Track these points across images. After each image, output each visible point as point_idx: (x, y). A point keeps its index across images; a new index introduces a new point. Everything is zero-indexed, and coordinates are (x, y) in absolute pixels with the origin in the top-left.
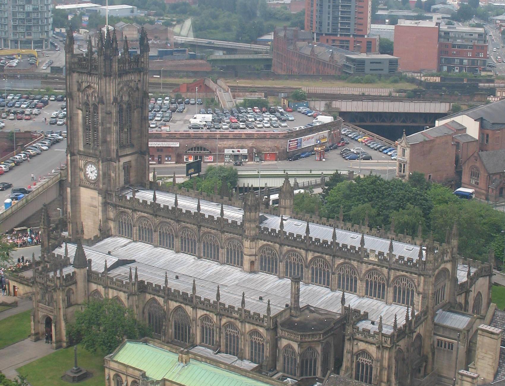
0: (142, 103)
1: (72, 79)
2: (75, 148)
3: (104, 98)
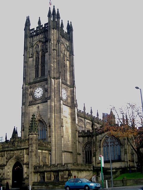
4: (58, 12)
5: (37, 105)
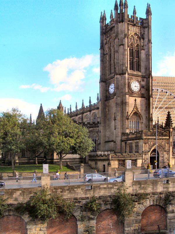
5: (134, 98)
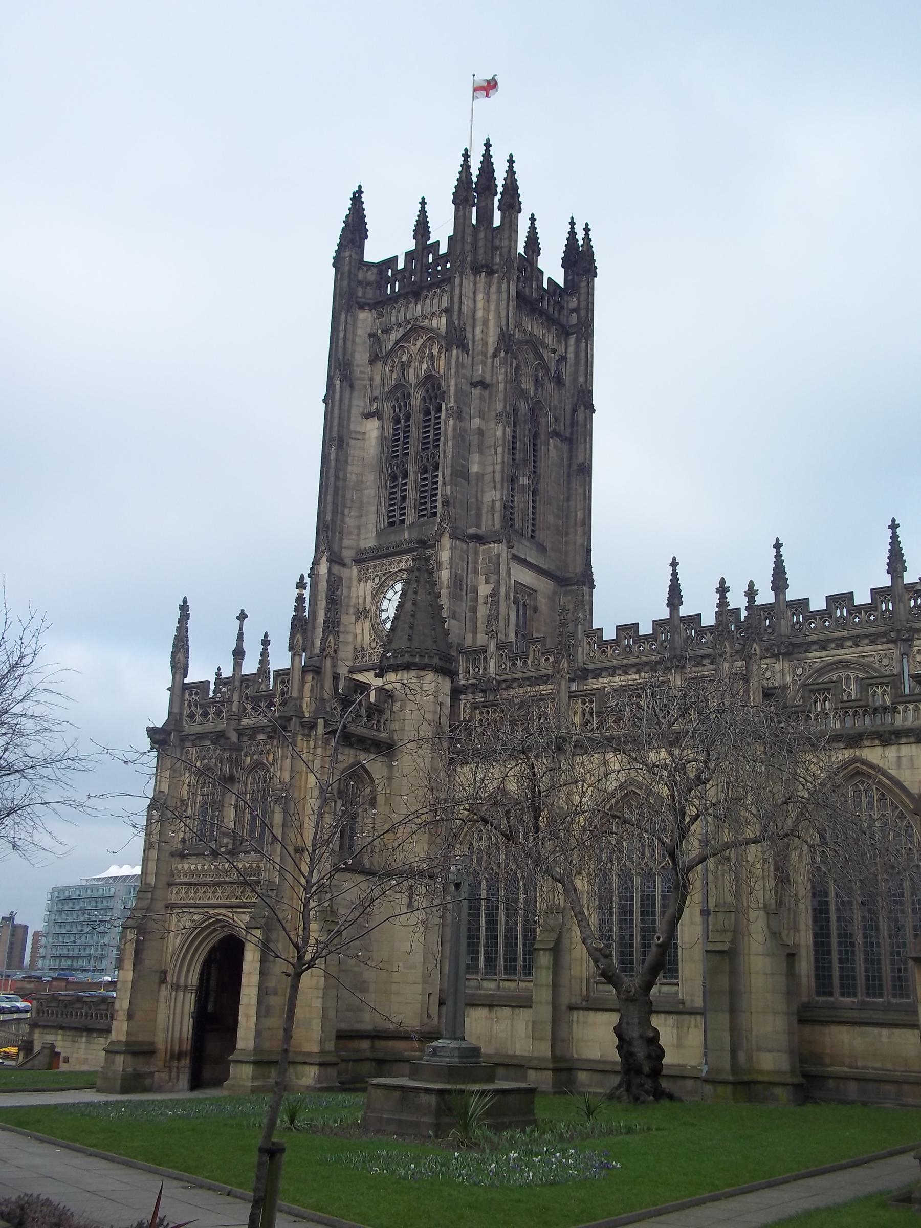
0: (574, 423)
1: (355, 325)
2: (346, 543)
3: (469, 335)
4: (511, 172)
